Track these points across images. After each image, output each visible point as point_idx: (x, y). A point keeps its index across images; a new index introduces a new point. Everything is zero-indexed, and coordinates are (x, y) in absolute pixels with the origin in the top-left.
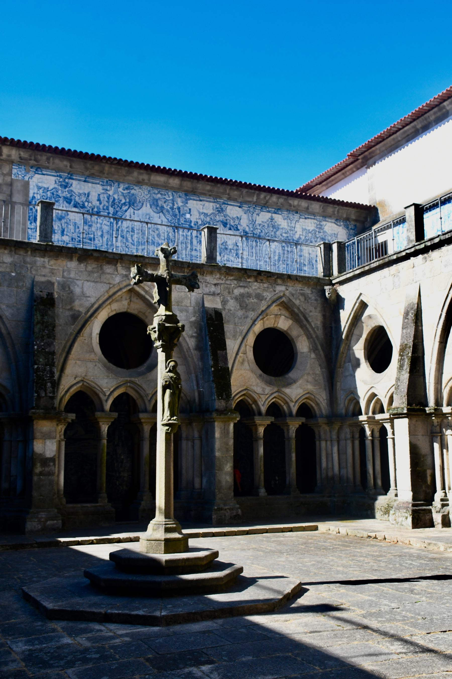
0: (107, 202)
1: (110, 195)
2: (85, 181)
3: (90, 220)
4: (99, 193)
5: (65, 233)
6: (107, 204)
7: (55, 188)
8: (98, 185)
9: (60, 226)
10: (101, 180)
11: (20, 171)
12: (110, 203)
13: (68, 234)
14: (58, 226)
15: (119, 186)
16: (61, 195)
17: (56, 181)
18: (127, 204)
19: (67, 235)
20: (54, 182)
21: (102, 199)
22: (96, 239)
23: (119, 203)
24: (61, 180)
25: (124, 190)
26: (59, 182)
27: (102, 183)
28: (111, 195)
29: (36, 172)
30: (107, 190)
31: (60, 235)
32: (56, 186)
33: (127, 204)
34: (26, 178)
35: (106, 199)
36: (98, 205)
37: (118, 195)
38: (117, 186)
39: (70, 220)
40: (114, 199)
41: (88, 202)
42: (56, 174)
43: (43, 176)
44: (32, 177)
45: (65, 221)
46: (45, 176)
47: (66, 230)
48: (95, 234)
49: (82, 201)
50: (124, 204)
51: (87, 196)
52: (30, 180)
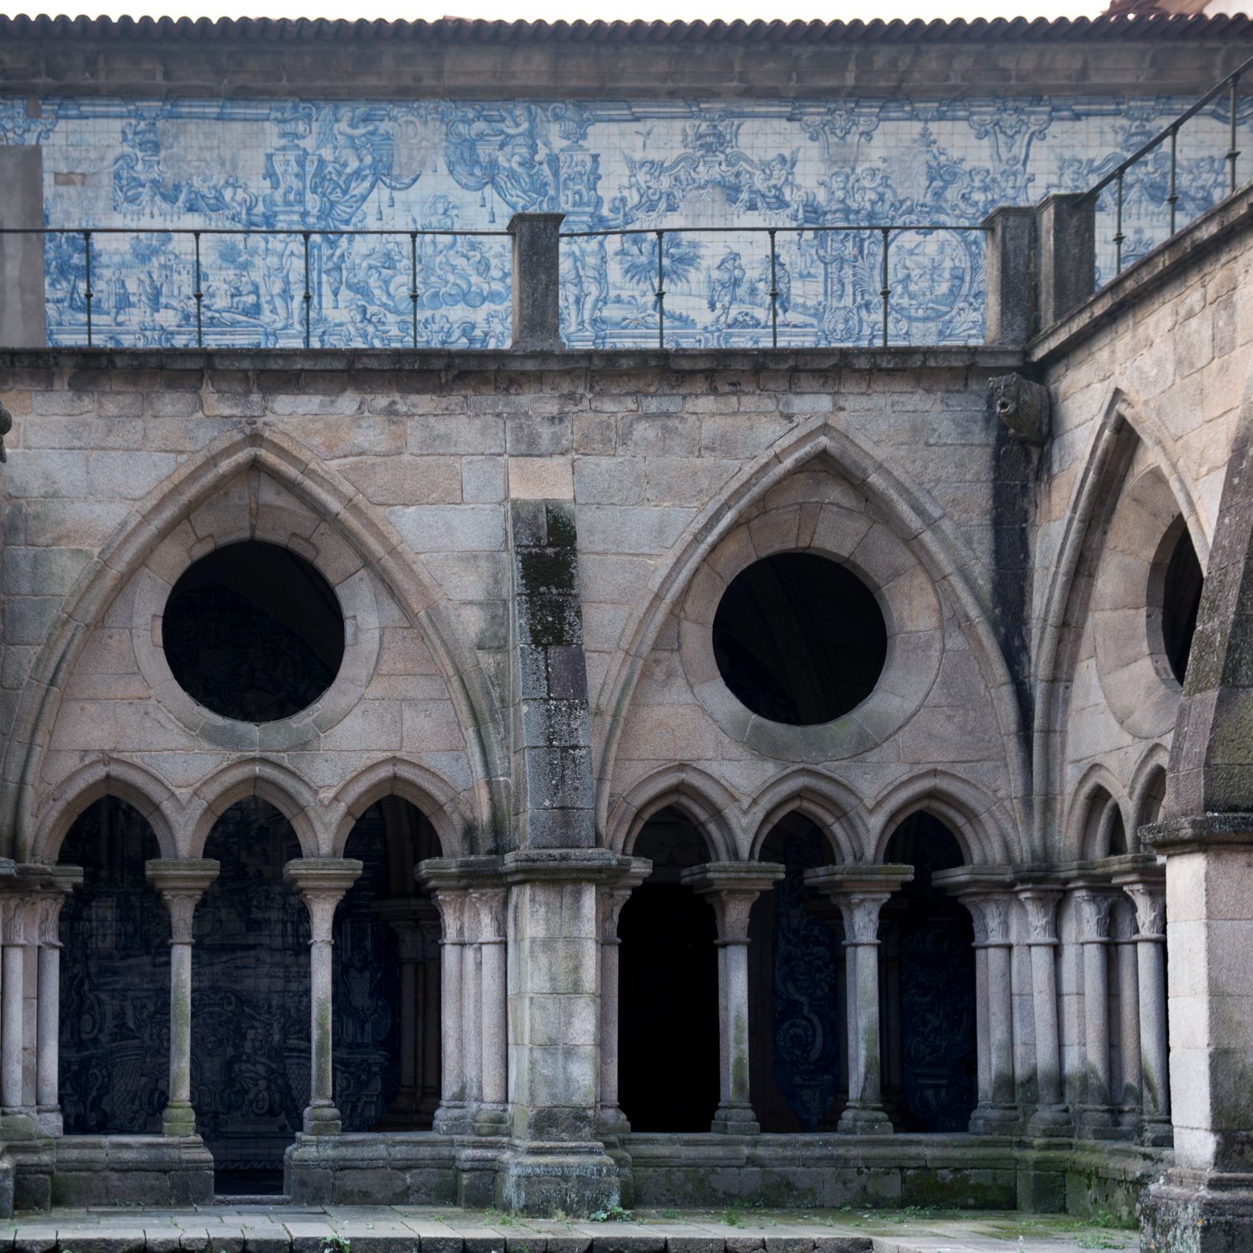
0: (297, 175)
1: (306, 153)
2: (220, 118)
3: (242, 246)
4: (270, 151)
5: (163, 300)
6: (296, 184)
7: (123, 157)
8: (267, 124)
9: (147, 281)
10: (274, 104)
11: (12, 118)
12: (309, 178)
13: (174, 303)
14: (141, 281)
15: (335, 115)
16: (142, 177)
17: (124, 133)
18: (367, 172)
19: (166, 307)
20: (119, 136)
21: (279, 169)
22: (266, 308)
23: (339, 174)
24: (142, 125)
25: (353, 125)
26: (136, 133)
27: (279, 115)
28: (310, 151)
29: (62, 113)
30: (296, 136)
31: (148, 310)
32: (127, 149)
33: (367, 172)
34: (31, 139)
35: (294, 168)
36: (268, 191)
37: (335, 148)
38: (330, 117)
39: (176, 257)
40: (322, 162)
41: (235, 187)
42: (124, 109)
43: (84, 122)
44: (49, 131)
45: (162, 260)
46: (91, 121)
47: (164, 290)
48: (262, 291)
49: (215, 187)
50: (357, 174)
51: (228, 164)
52: (42, 141)
